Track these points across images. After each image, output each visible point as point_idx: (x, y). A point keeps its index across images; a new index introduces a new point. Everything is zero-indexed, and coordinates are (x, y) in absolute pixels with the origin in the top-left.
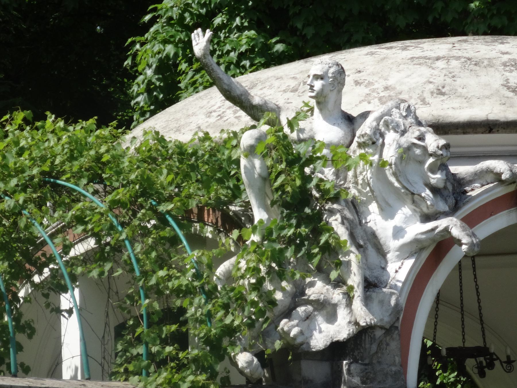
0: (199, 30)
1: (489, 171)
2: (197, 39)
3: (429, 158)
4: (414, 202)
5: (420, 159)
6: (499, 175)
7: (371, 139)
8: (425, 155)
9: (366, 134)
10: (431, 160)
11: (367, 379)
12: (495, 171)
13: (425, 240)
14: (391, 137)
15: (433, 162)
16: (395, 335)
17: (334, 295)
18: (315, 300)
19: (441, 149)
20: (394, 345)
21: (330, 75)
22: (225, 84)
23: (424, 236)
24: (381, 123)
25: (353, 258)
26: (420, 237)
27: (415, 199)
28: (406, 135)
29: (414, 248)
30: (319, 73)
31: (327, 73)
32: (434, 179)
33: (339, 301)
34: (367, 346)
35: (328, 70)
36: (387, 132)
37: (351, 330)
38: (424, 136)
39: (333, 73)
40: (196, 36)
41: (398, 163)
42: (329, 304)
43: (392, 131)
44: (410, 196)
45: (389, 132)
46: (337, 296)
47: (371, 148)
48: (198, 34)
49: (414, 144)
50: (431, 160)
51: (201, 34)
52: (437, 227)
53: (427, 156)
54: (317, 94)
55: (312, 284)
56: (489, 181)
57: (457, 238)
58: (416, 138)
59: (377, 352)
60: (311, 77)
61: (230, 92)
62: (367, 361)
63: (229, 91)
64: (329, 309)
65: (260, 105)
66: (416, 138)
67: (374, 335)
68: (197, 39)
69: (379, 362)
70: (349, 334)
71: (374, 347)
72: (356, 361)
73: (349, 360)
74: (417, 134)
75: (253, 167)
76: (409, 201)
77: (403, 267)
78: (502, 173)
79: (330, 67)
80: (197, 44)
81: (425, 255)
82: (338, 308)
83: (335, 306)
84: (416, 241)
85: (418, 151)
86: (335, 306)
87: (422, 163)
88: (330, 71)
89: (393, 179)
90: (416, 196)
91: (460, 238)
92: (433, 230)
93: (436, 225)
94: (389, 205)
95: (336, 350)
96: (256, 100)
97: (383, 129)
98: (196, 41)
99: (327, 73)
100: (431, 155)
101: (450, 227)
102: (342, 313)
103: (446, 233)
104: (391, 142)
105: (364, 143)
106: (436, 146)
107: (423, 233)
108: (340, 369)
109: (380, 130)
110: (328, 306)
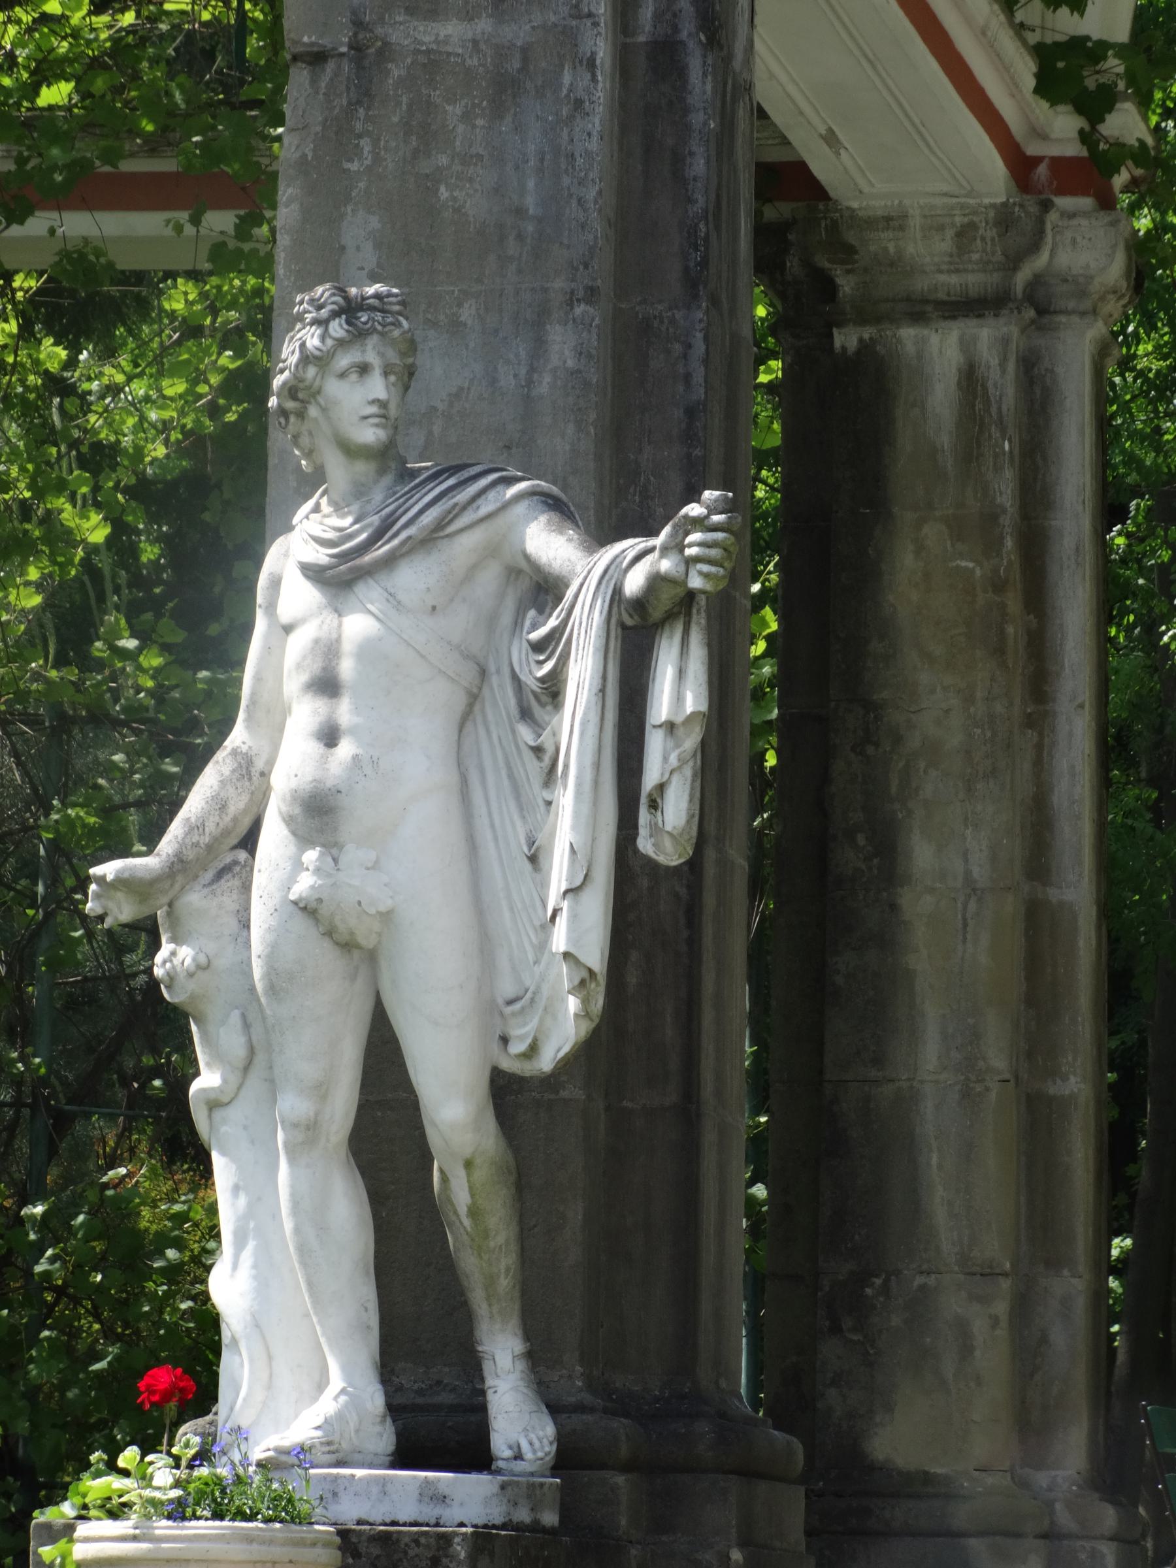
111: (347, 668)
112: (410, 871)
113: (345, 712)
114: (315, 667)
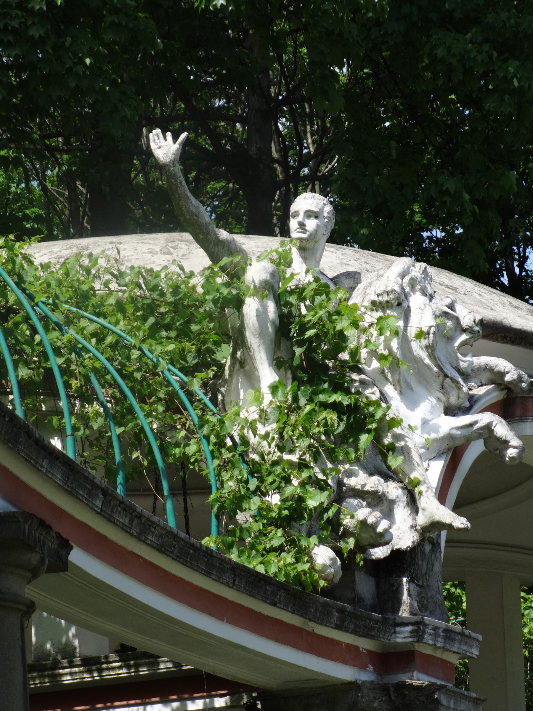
0: (158, 131)
1: (487, 369)
2: (157, 141)
3: (461, 334)
4: (443, 387)
5: (451, 333)
6: (502, 374)
7: (398, 298)
8: (456, 330)
9: (393, 290)
10: (464, 337)
11: (422, 605)
12: (496, 369)
13: (461, 437)
14: (416, 301)
15: (467, 339)
17: (390, 490)
18: (373, 491)
19: (477, 325)
21: (326, 215)
22: (193, 205)
23: (458, 432)
24: (406, 280)
26: (454, 432)
27: (445, 384)
28: (433, 301)
29: (444, 446)
30: (316, 209)
31: (322, 210)
32: (465, 361)
33: (398, 497)
34: (420, 562)
35: (323, 208)
36: (412, 293)
37: (415, 537)
38: (454, 306)
39: (329, 213)
40: (156, 137)
41: (437, 332)
42: (387, 499)
43: (418, 294)
44: (441, 378)
45: (414, 294)
46: (393, 490)
47: (395, 310)
48: (158, 136)
49: (445, 313)
50: (464, 337)
51: (161, 135)
52: (476, 422)
53: (458, 332)
54: (310, 235)
55: (350, 474)
56: (484, 382)
57: (504, 438)
58: (447, 306)
59: (426, 573)
60: (302, 214)
61: (198, 217)
62: (420, 583)
63: (196, 216)
64: (386, 504)
65: (228, 241)
66: (447, 306)
67: (424, 549)
68: (157, 141)
69: (428, 586)
70: (413, 542)
73: (407, 577)
74: (448, 301)
75: (265, 308)
76: (436, 385)
77: (430, 469)
78: (508, 373)
79: (325, 205)
80: (160, 148)
82: (395, 506)
83: (392, 503)
85: (449, 324)
86: (392, 503)
87: (450, 339)
88: (325, 209)
89: (423, 355)
90: (448, 380)
91: (508, 439)
92: (471, 425)
93: (476, 419)
94: (411, 389)
97: (407, 289)
98: (156, 144)
99: (322, 210)
100: (464, 331)
101: (494, 425)
102: (401, 512)
103: (486, 431)
104: (423, 307)
105: (387, 302)
106: (472, 319)
107: (458, 428)
108: (394, 588)
109: (404, 290)
110: (385, 502)
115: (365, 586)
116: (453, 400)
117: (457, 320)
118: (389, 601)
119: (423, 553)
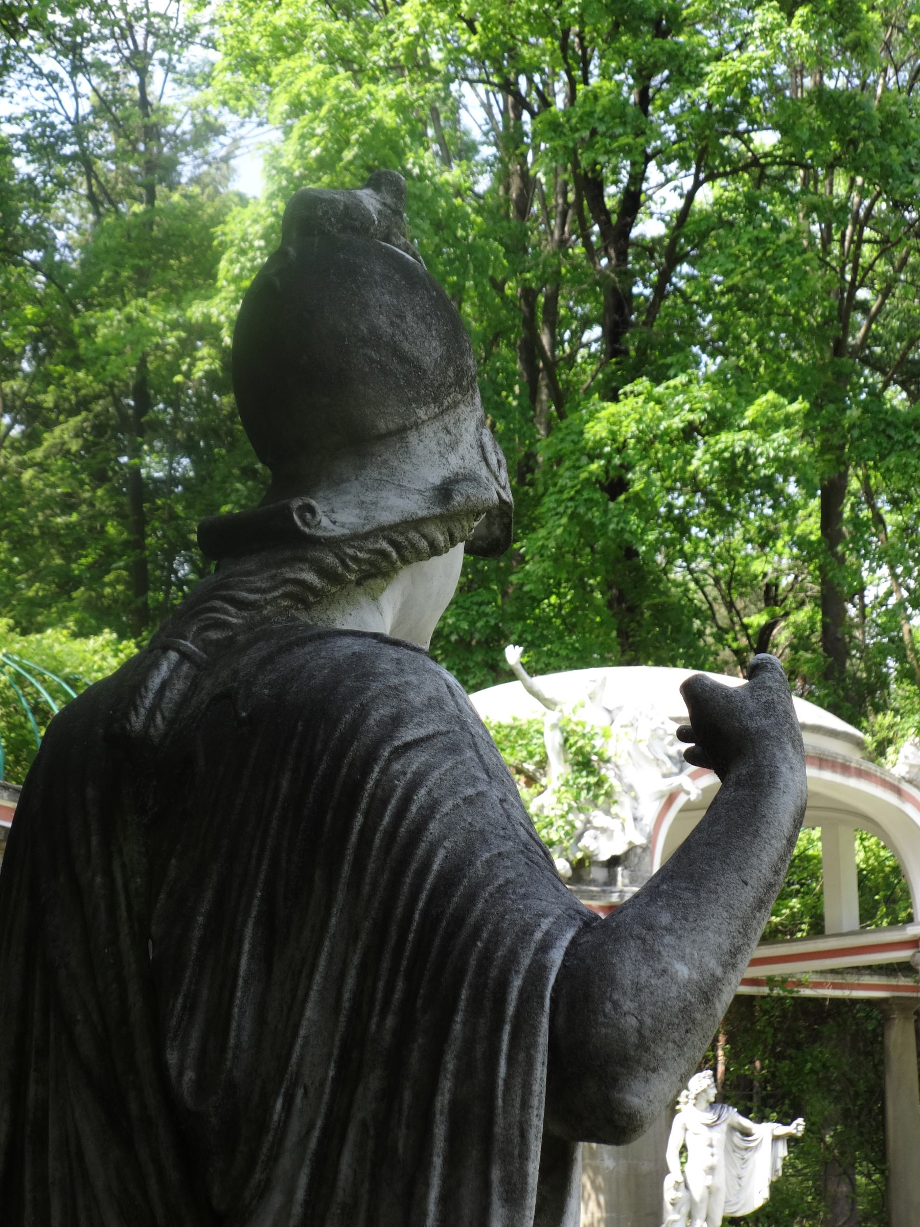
16: (648, 852)
20: (647, 859)
25: (626, 800)
71: (636, 860)
72: (626, 868)
81: (664, 800)
84: (661, 791)
87: (662, 739)
95: (614, 862)
96: (547, 695)
111: (714, 1143)
112: (720, 1179)
113: (714, 1150)
114: (708, 1143)
115: (599, 874)
116: (665, 771)
117: (665, 731)
118: (611, 881)
119: (635, 854)
